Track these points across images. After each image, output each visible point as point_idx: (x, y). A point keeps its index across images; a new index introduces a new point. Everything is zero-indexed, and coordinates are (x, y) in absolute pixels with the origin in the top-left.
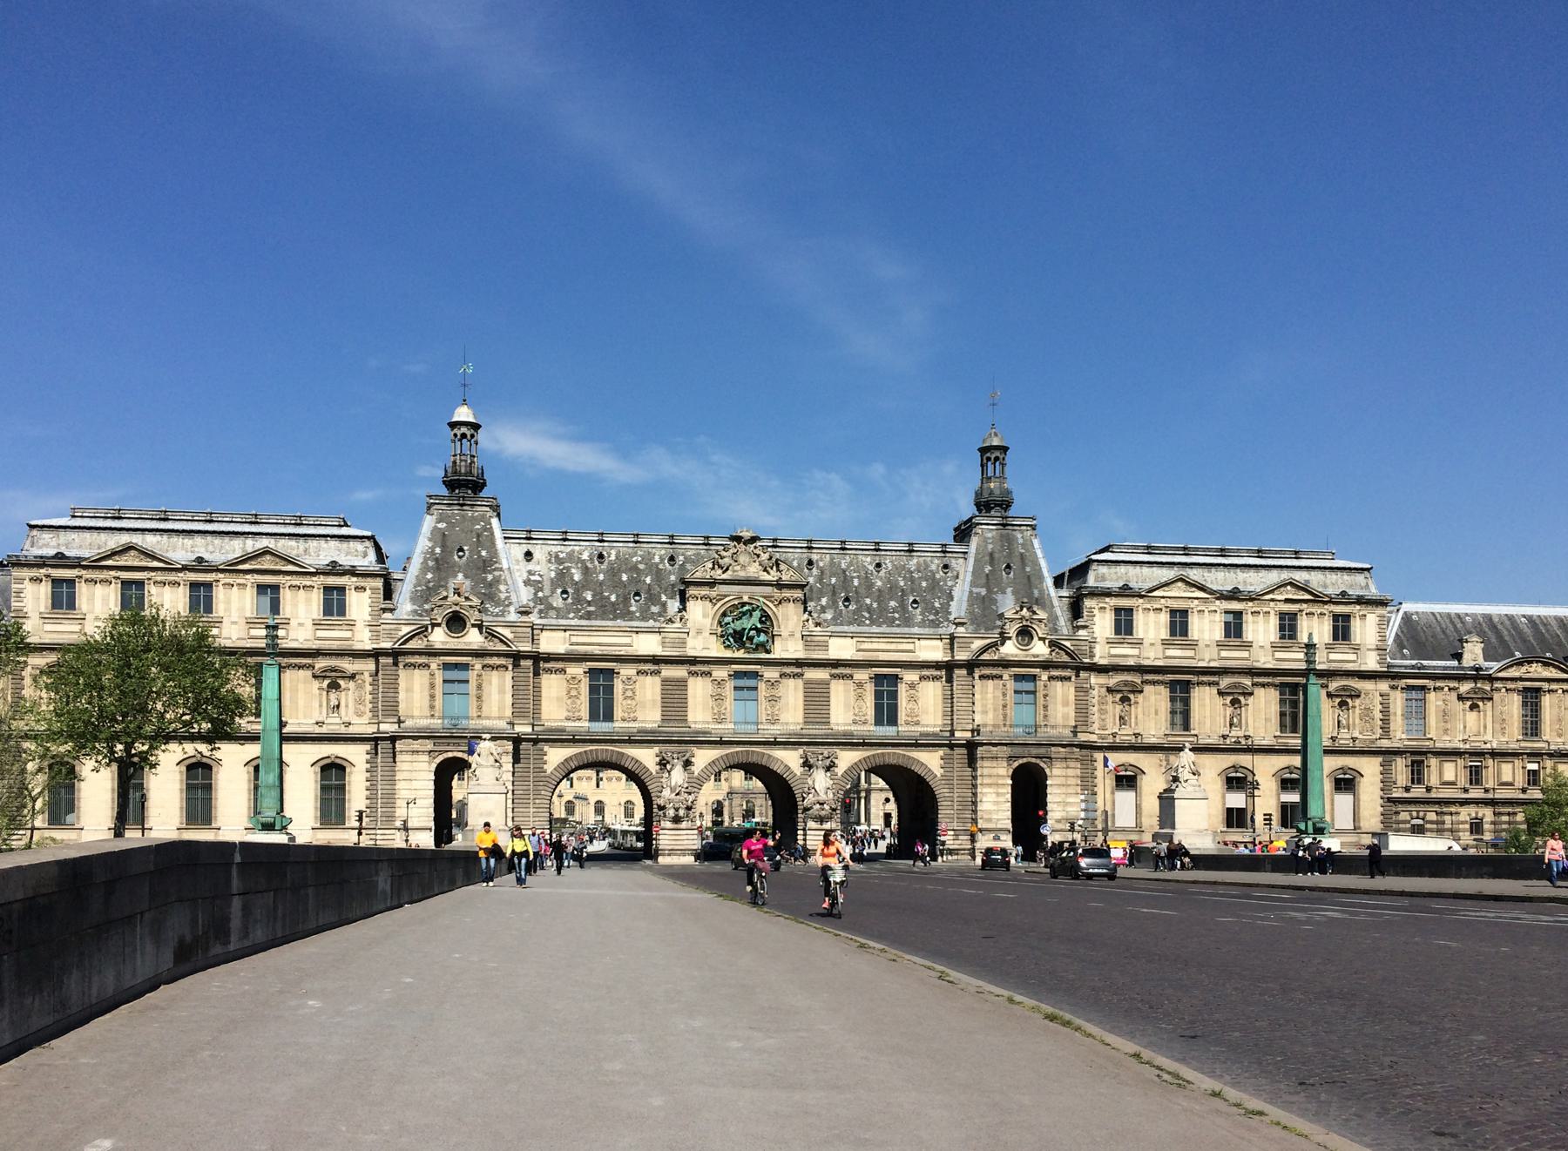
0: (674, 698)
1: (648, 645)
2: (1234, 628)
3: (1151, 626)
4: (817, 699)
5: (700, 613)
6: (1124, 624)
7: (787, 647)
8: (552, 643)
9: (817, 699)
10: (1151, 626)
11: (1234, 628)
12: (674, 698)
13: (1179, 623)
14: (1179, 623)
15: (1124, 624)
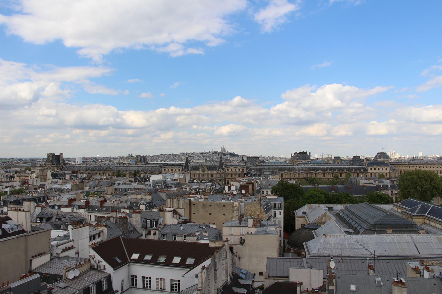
0: (199, 175)
1: (197, 172)
2: (235, 170)
3: (230, 170)
4: (208, 175)
5: (200, 170)
6: (228, 170)
7: (206, 172)
8: (192, 172)
9: (208, 175)
10: (230, 170)
11: (235, 170)
12: (199, 175)
13: (232, 170)
14: (232, 170)
15: (228, 170)
